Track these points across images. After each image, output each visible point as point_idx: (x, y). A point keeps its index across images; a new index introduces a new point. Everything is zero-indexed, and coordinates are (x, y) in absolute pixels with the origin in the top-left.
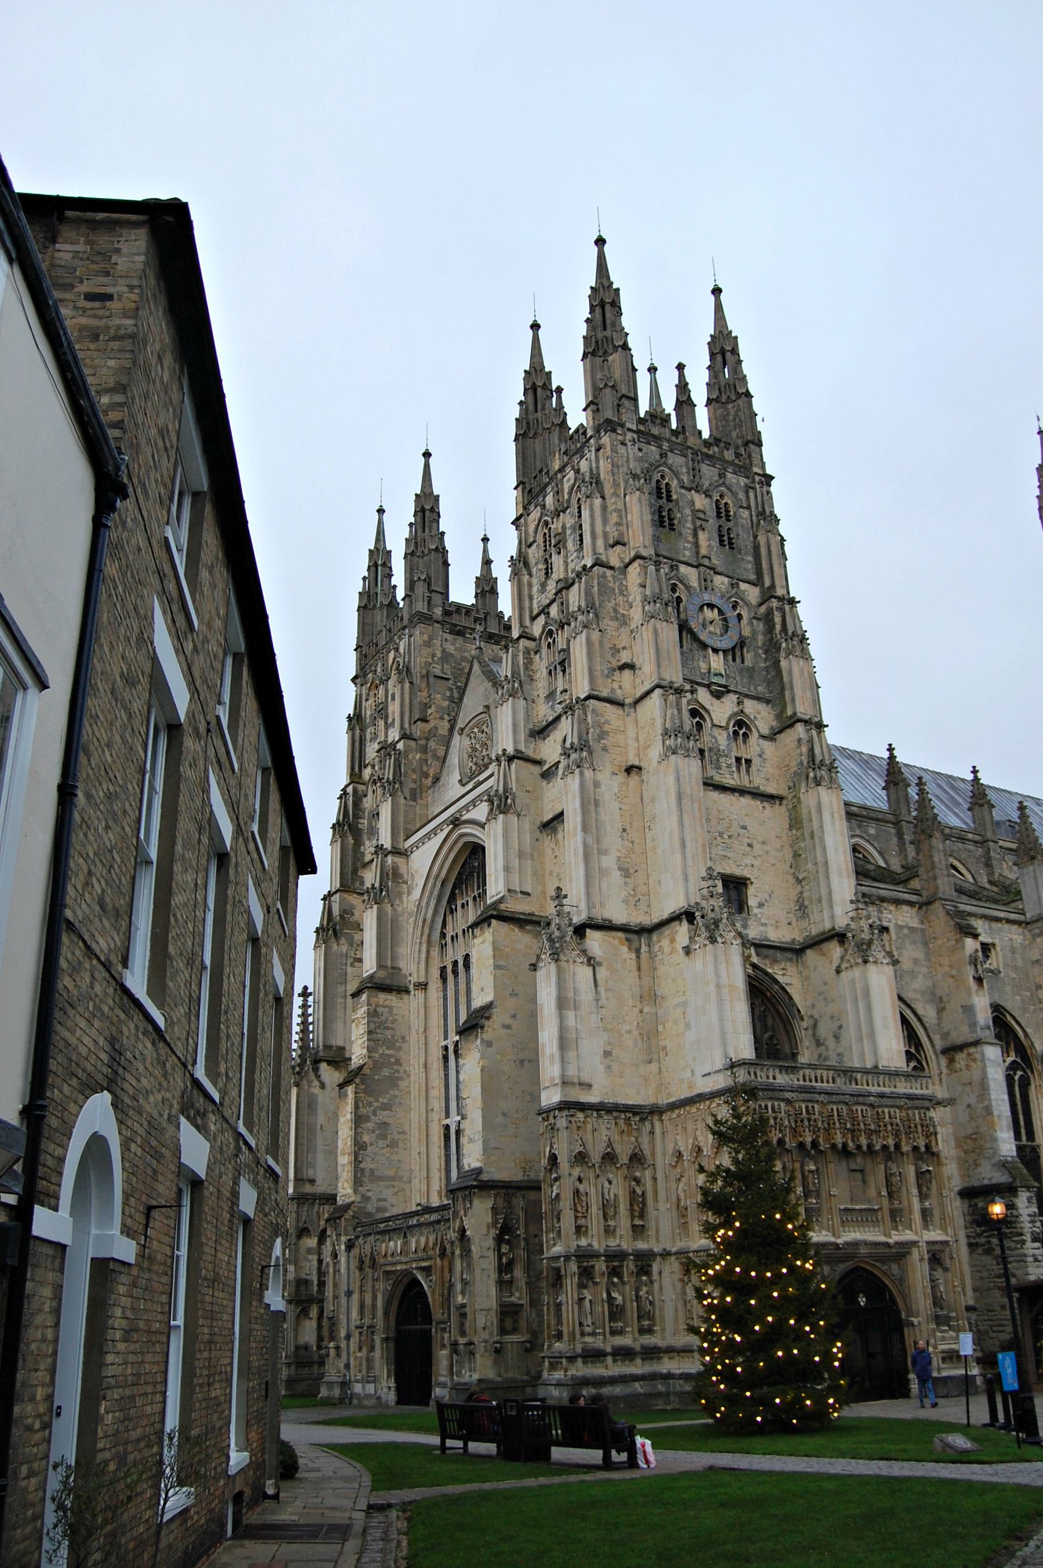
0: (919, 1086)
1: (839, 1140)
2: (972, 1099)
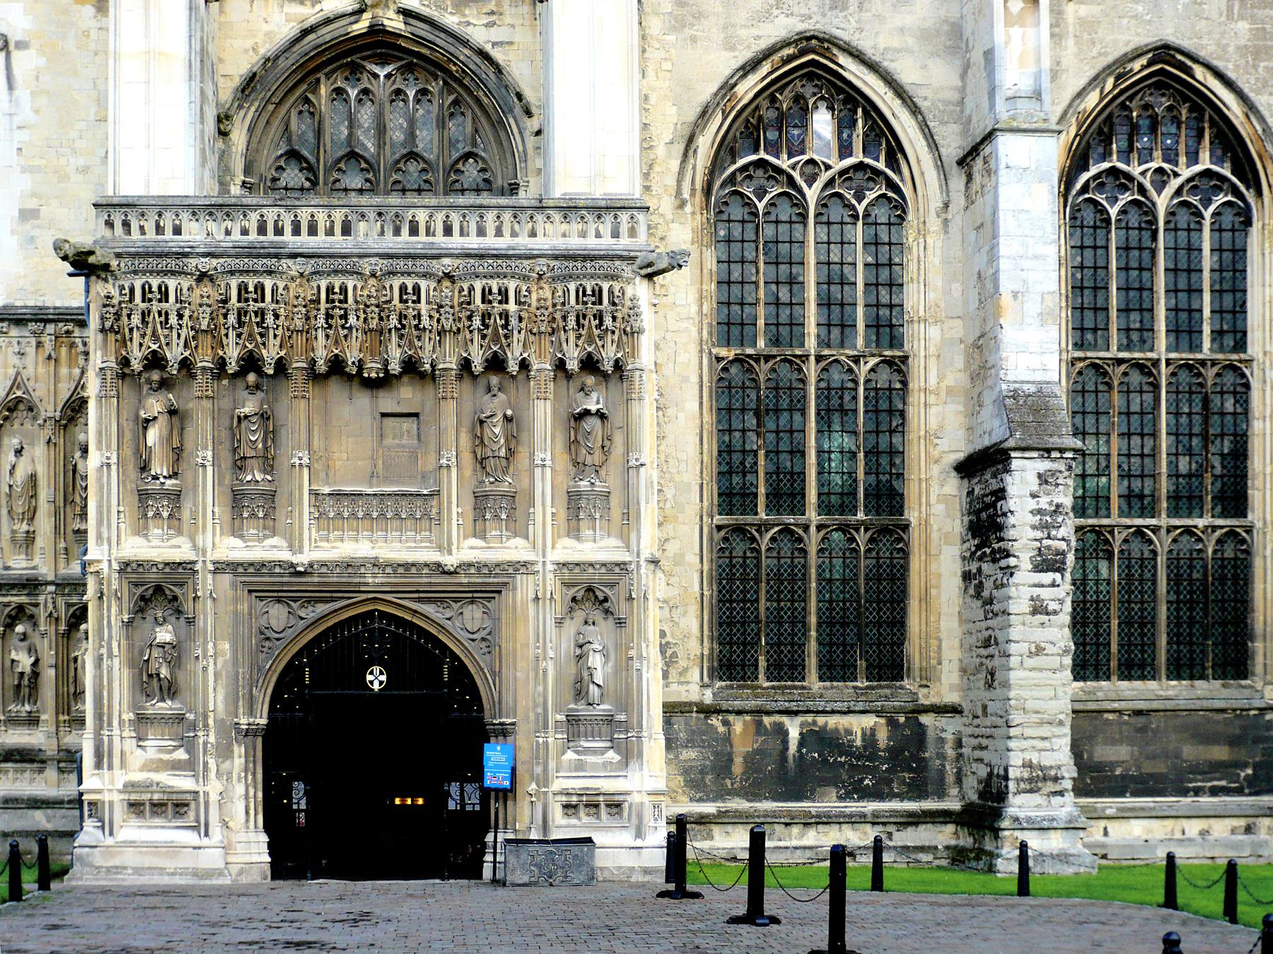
0: (606, 228)
1: (322, 352)
2: (980, 260)
